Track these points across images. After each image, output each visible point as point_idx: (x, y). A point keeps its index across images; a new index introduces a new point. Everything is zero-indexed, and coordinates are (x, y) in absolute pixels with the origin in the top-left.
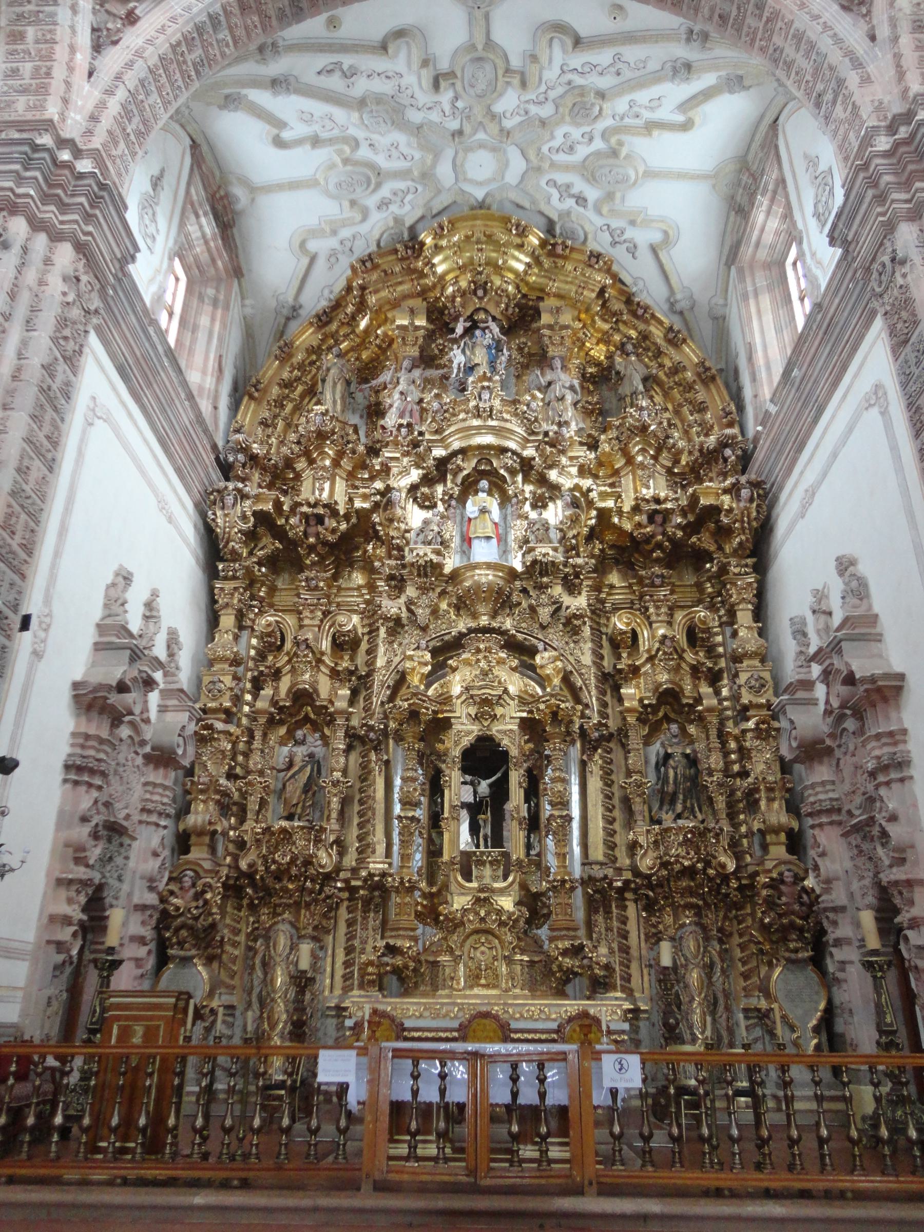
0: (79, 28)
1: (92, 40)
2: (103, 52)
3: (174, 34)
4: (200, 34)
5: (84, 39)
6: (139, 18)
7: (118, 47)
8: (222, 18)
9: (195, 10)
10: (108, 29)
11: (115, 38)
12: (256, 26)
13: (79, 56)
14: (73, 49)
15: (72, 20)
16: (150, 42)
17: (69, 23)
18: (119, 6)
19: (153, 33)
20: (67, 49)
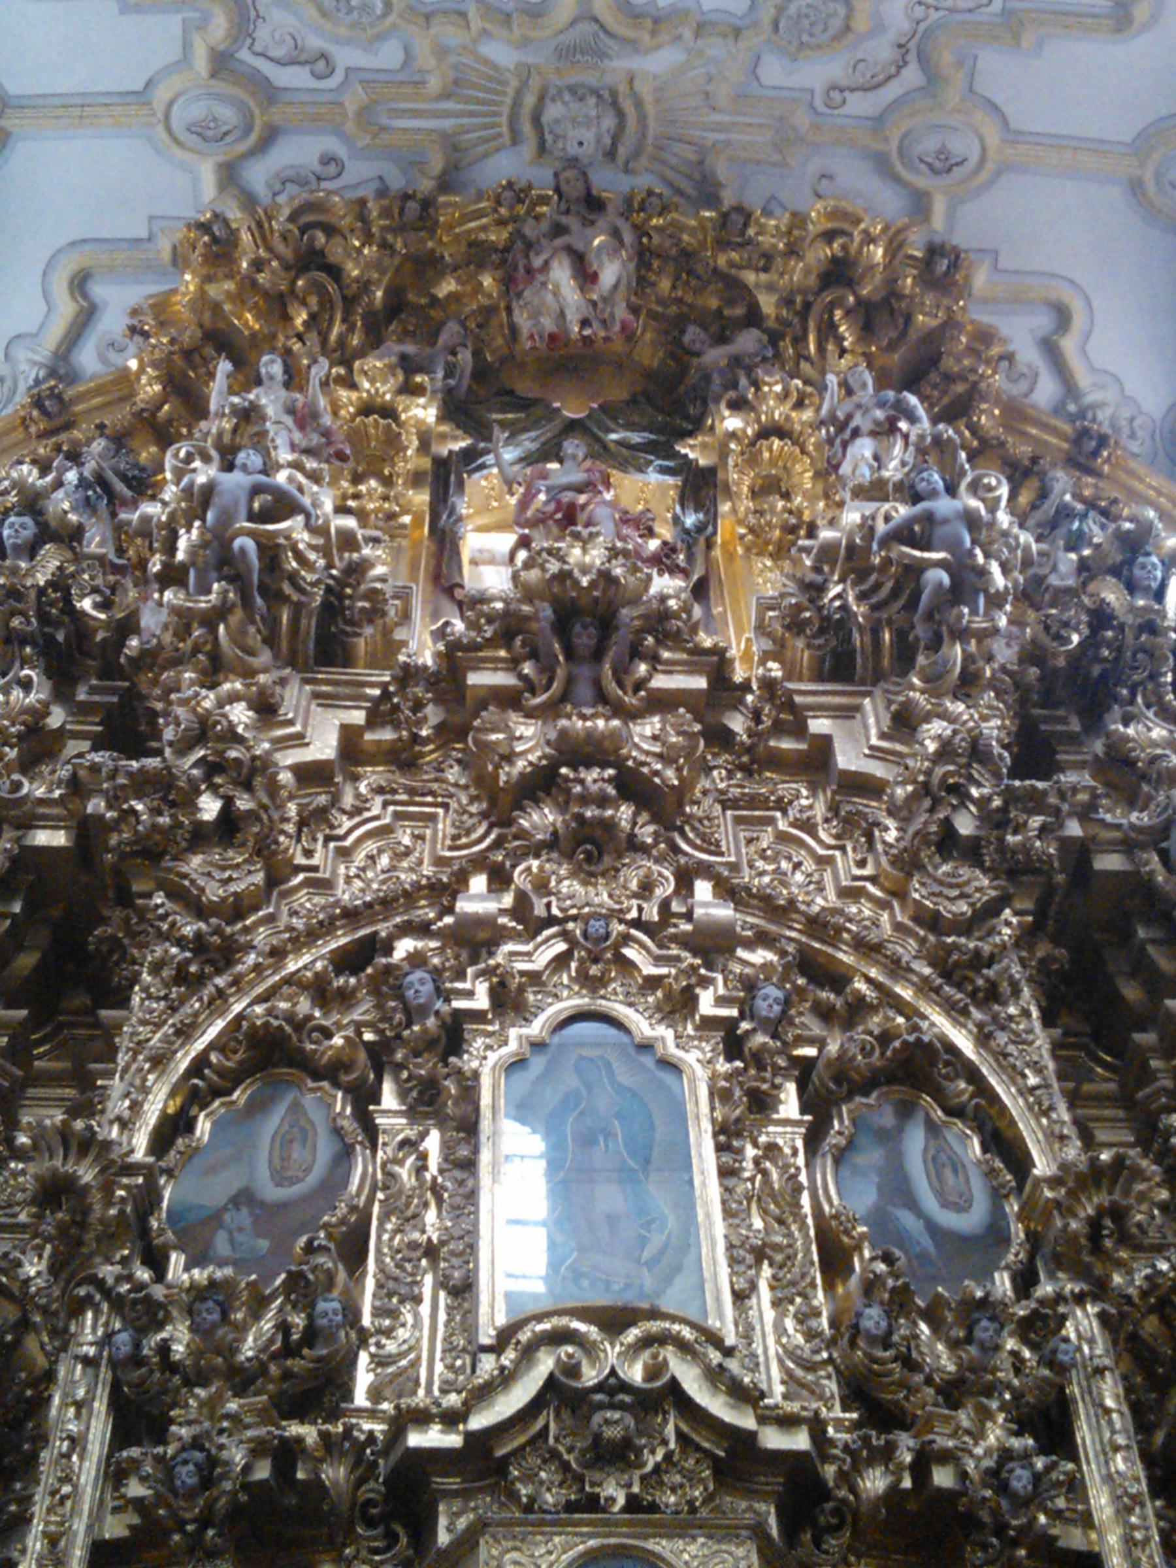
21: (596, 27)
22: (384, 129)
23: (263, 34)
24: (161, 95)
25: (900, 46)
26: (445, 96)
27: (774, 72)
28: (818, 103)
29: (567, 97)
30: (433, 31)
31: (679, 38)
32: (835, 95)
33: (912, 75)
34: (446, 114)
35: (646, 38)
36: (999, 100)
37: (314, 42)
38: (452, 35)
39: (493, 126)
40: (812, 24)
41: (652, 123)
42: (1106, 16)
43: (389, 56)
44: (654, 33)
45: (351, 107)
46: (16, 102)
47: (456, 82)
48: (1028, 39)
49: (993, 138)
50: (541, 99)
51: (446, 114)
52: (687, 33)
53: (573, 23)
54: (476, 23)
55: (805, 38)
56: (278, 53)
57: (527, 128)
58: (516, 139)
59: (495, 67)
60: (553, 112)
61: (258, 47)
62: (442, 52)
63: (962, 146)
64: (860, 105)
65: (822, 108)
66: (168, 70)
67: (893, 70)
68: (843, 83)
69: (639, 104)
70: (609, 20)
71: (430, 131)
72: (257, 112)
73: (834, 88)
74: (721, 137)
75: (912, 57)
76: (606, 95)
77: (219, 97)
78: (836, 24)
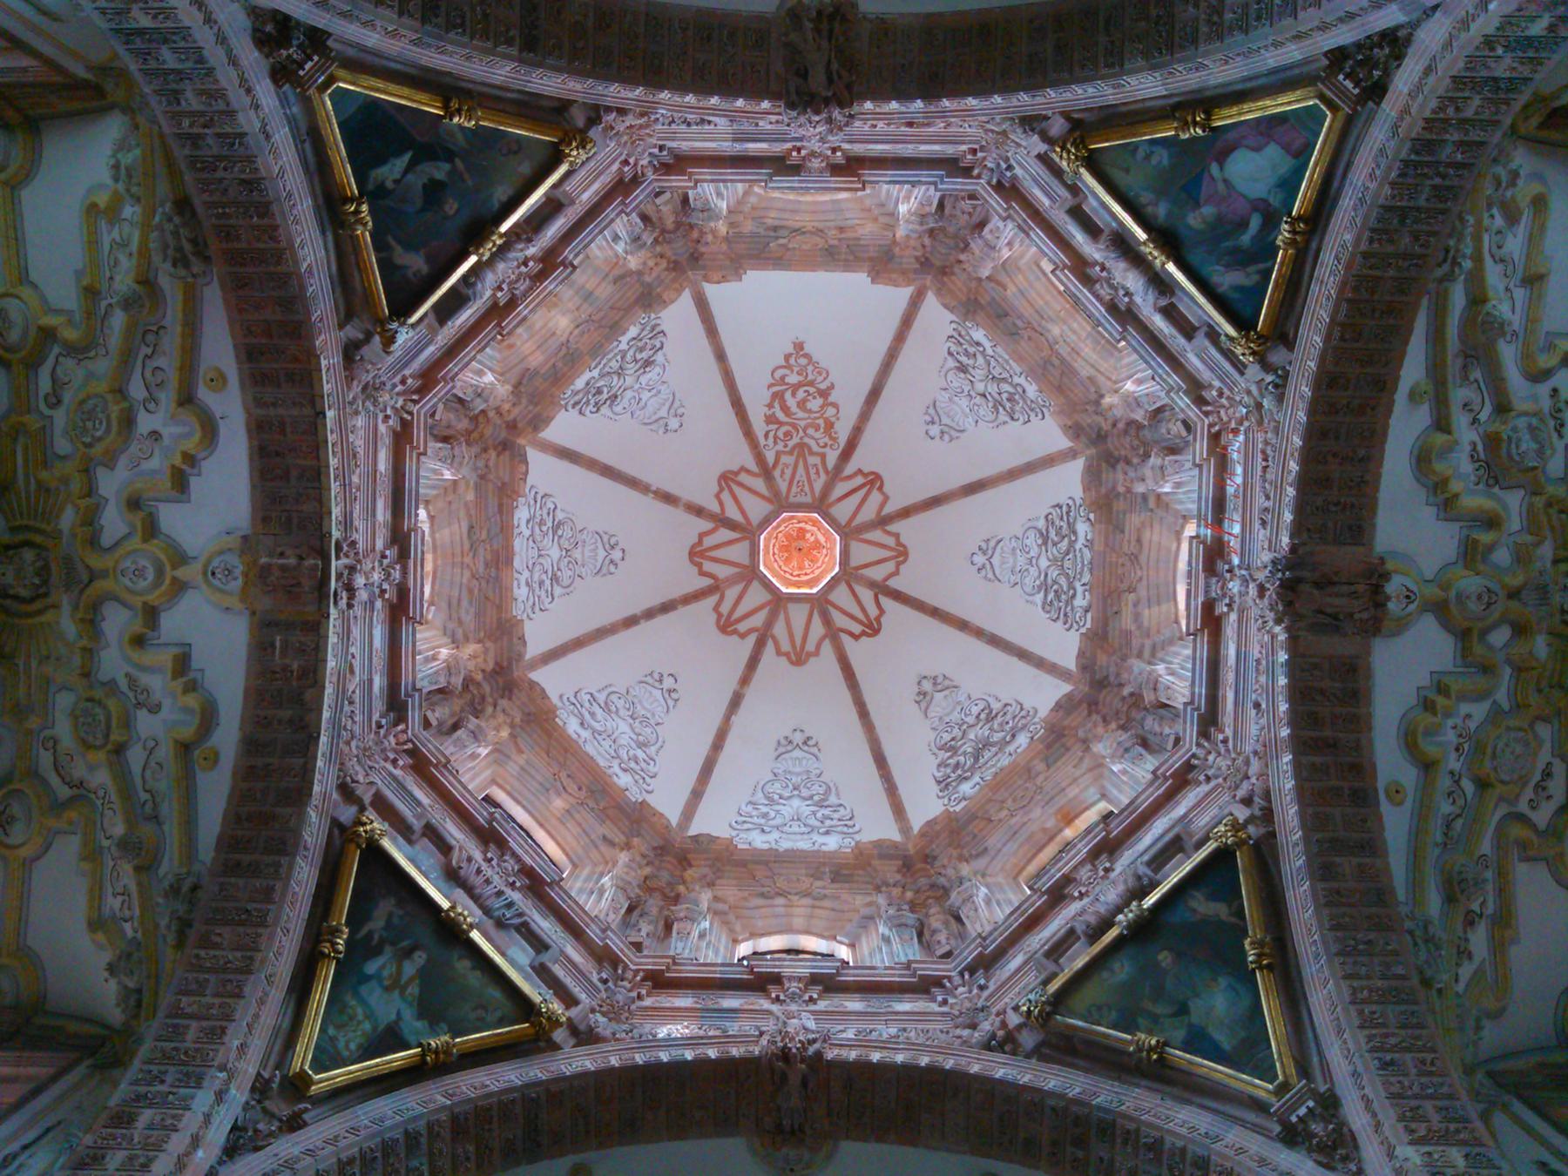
0: (216, 1120)
1: (228, 1139)
2: (237, 1158)
3: (350, 1146)
4: (386, 1155)
5: (218, 1135)
6: (305, 1124)
7: (261, 1153)
8: (423, 1140)
9: (388, 1123)
10: (256, 1131)
11: (260, 1143)
12: (468, 1159)
13: (200, 1153)
14: (196, 1141)
15: (212, 1107)
16: (310, 1152)
17: (206, 1109)
18: (283, 1106)
19: (319, 1144)
20: (188, 1140)
21: (86, 581)
22: (15, 440)
23: (69, 363)
24: (26, 292)
25: (81, 783)
26: (40, 484)
27: (64, 701)
28: (48, 733)
29: (38, 564)
30: (76, 474)
31: (81, 637)
32: (51, 744)
33: (64, 792)
34: (28, 484)
35: (80, 615)
36: (50, 852)
37: (67, 397)
38: (76, 486)
39: (21, 514)
40: (89, 724)
41: (30, 621)
42: (100, 915)
43: (62, 446)
44: (82, 620)
45: (26, 419)
46: (16, 194)
47: (48, 490)
48: (86, 866)
49: (24, 852)
50: (39, 546)
51: (28, 484)
52: (84, 642)
53: (88, 567)
54: (83, 503)
55: (81, 719)
56: (59, 370)
57: (21, 537)
58: (14, 530)
59: (58, 517)
60: (28, 555)
61: (61, 359)
62: (65, 480)
63: (17, 833)
64: (46, 759)
65: (42, 735)
66: (44, 300)
67: (67, 780)
68: (58, 748)
69: (40, 612)
70: (88, 592)
71: (15, 472)
72: (18, 356)
73: (55, 742)
74: (21, 667)
75: (75, 791)
76: (42, 591)
77: (25, 333)
78: (91, 739)
